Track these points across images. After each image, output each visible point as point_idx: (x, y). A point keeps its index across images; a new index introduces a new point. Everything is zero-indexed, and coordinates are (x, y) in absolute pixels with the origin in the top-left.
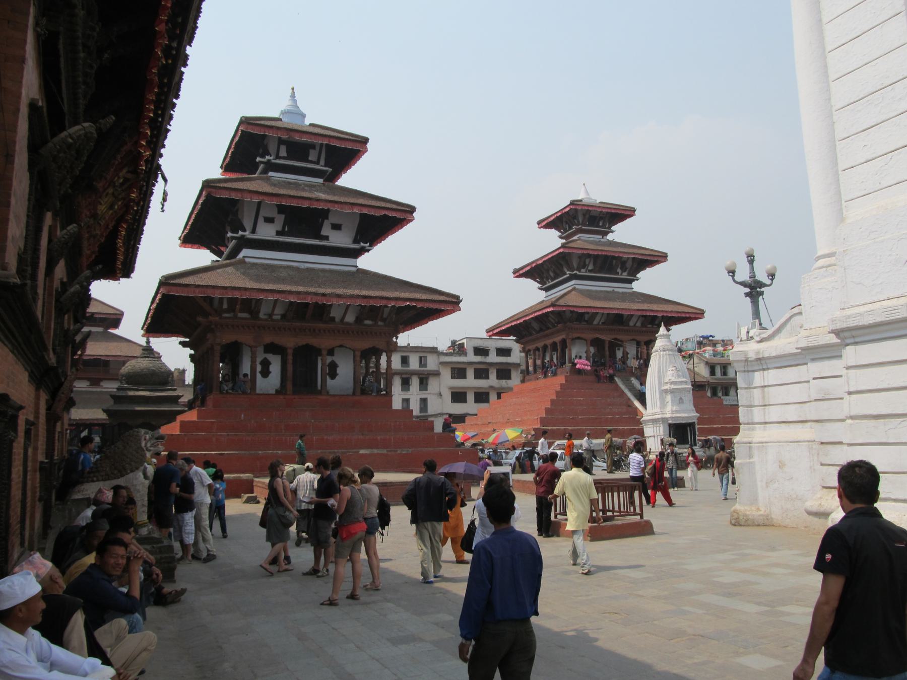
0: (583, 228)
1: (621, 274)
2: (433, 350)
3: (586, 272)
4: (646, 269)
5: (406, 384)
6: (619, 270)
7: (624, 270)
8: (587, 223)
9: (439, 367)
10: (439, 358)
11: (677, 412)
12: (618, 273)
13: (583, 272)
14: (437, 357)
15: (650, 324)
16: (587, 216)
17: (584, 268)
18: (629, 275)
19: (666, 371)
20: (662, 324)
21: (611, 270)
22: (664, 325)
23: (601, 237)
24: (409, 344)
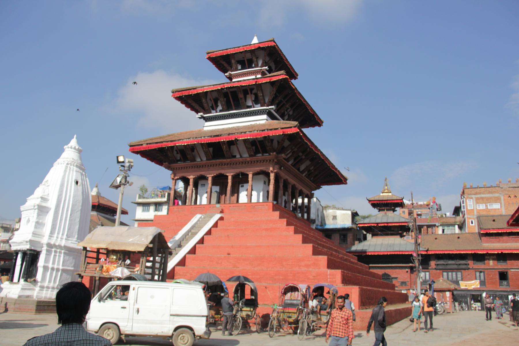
1: (254, 107)
3: (216, 112)
6: (250, 103)
8: (240, 67)
13: (213, 114)
18: (261, 106)
20: (75, 136)
22: (77, 138)
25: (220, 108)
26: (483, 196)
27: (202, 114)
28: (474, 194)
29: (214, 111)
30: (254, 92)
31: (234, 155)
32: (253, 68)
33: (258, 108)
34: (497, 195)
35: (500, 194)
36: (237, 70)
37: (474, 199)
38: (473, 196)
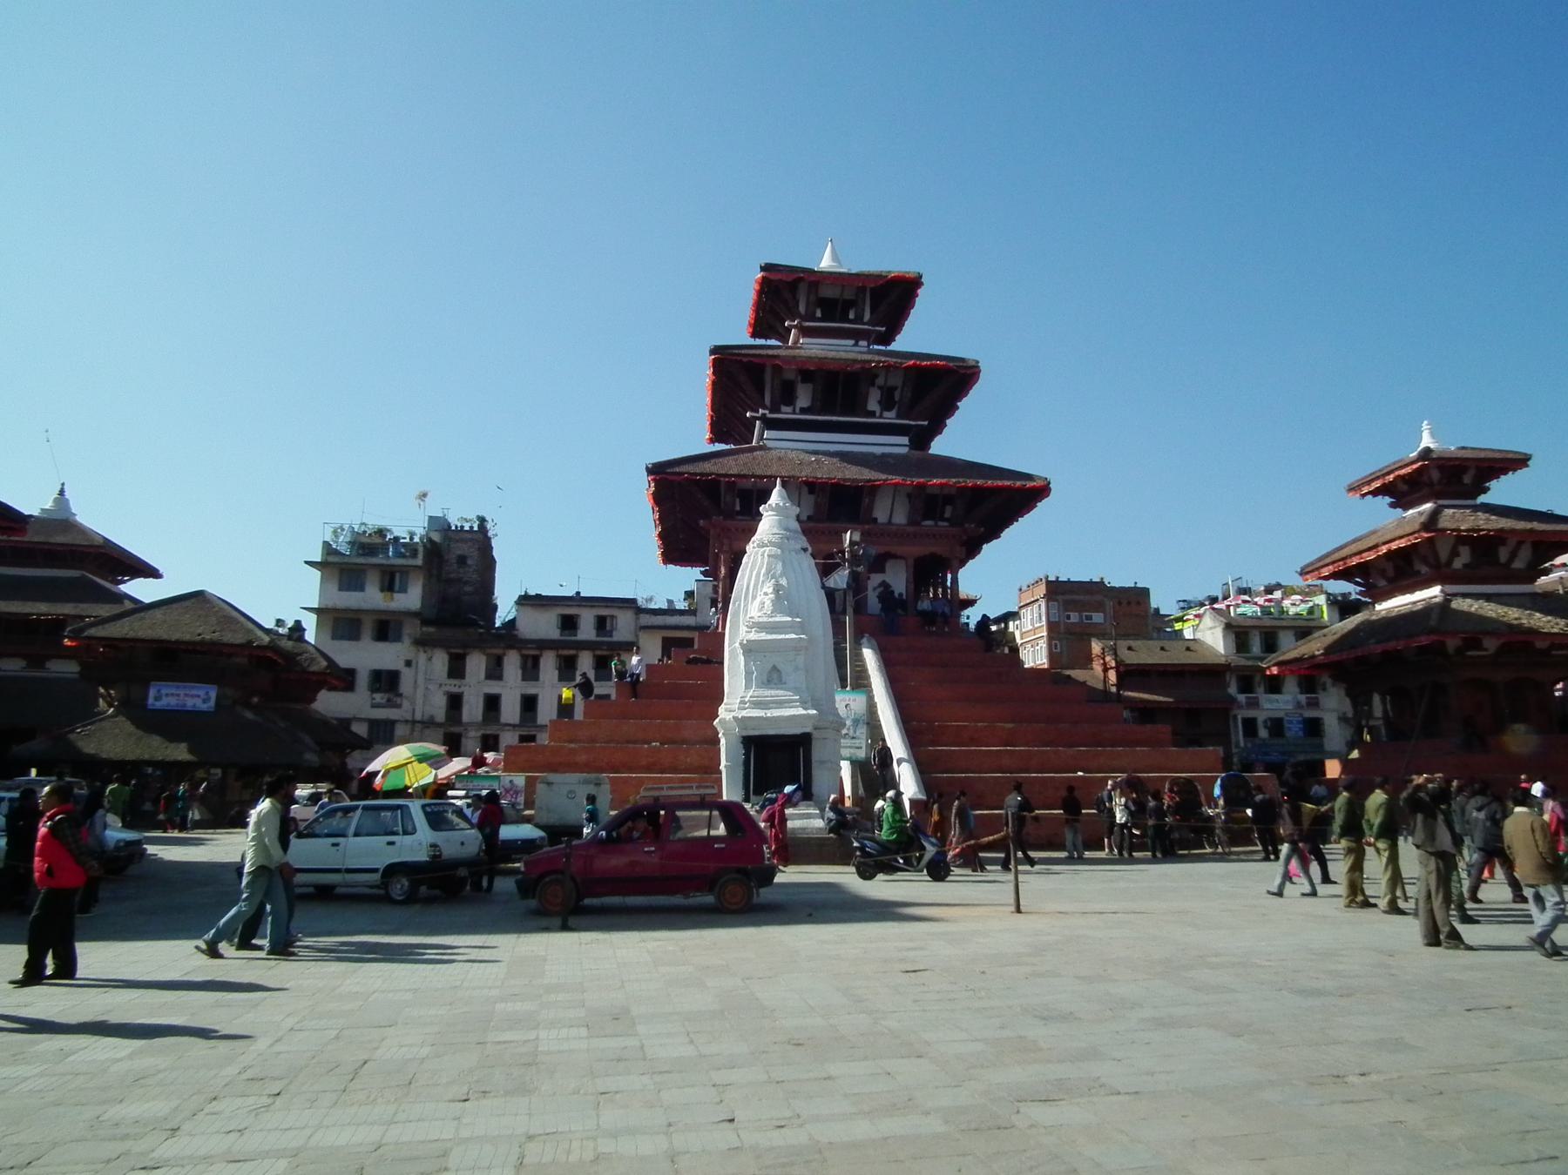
0: (807, 324)
1: (881, 417)
2: (629, 604)
3: (794, 413)
4: (958, 408)
5: (567, 668)
7: (887, 404)
8: (819, 314)
9: (637, 636)
10: (637, 619)
11: (758, 704)
12: (872, 414)
13: (786, 413)
14: (634, 616)
15: (925, 519)
16: (812, 298)
17: (787, 405)
18: (899, 416)
19: (754, 598)
21: (854, 404)
23: (851, 342)
24: (578, 593)
25: (803, 400)
26: (1076, 597)
27: (767, 412)
28: (1063, 594)
29: (789, 409)
30: (880, 381)
31: (874, 516)
32: (850, 322)
33: (890, 417)
34: (1098, 597)
35: (1106, 596)
36: (814, 319)
37: (1060, 600)
38: (1060, 598)
